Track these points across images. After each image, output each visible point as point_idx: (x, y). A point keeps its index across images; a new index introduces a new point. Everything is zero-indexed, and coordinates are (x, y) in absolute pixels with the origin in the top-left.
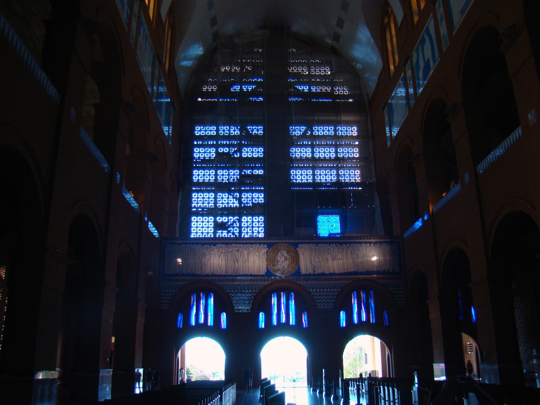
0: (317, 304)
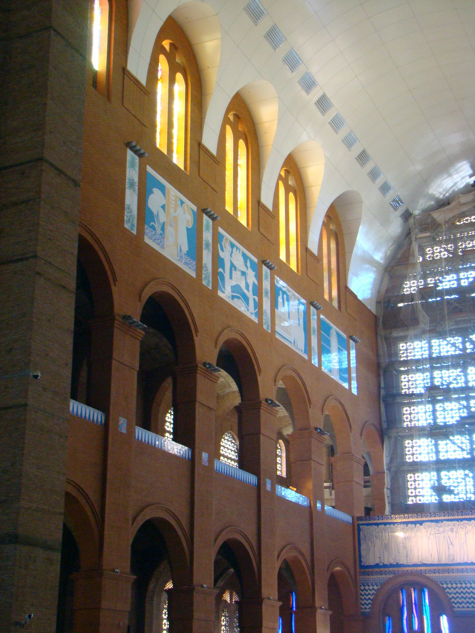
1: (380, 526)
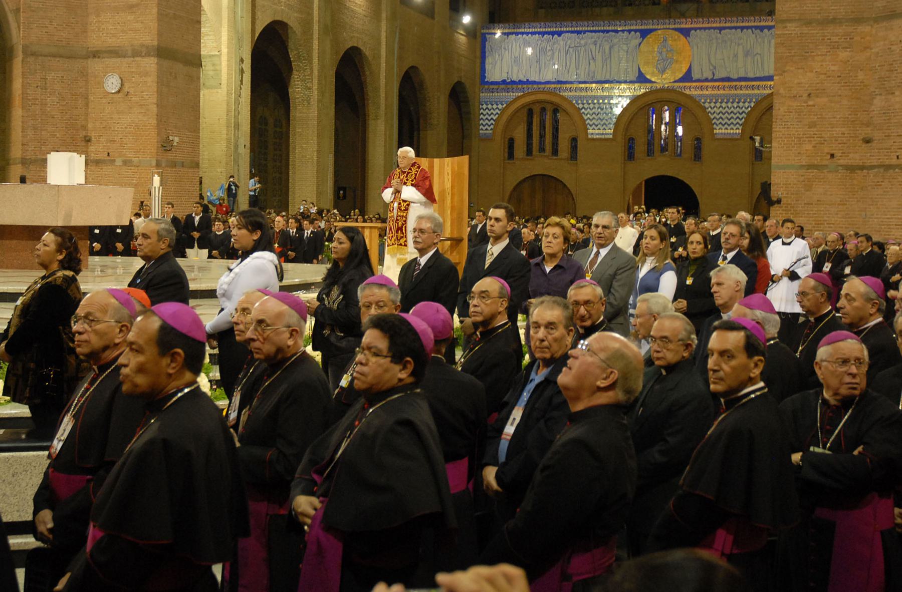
0: (715, 126)
1: (510, 36)
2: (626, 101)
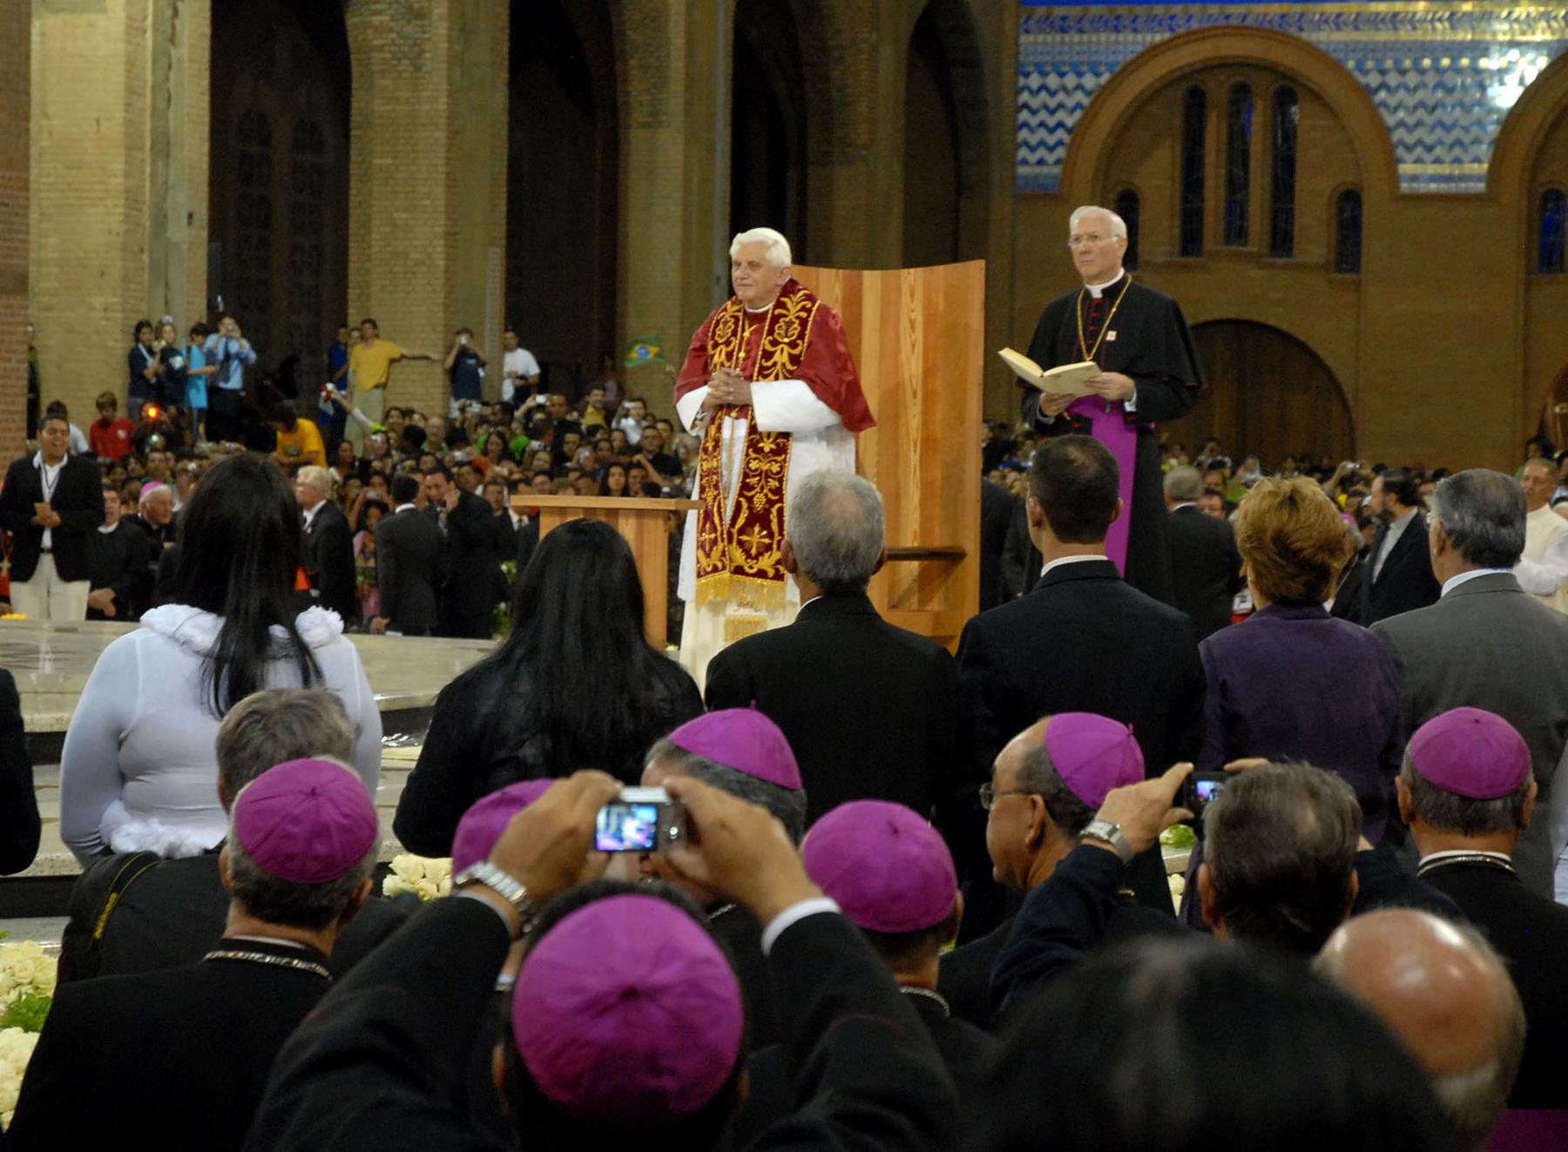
2: (1533, 62)
